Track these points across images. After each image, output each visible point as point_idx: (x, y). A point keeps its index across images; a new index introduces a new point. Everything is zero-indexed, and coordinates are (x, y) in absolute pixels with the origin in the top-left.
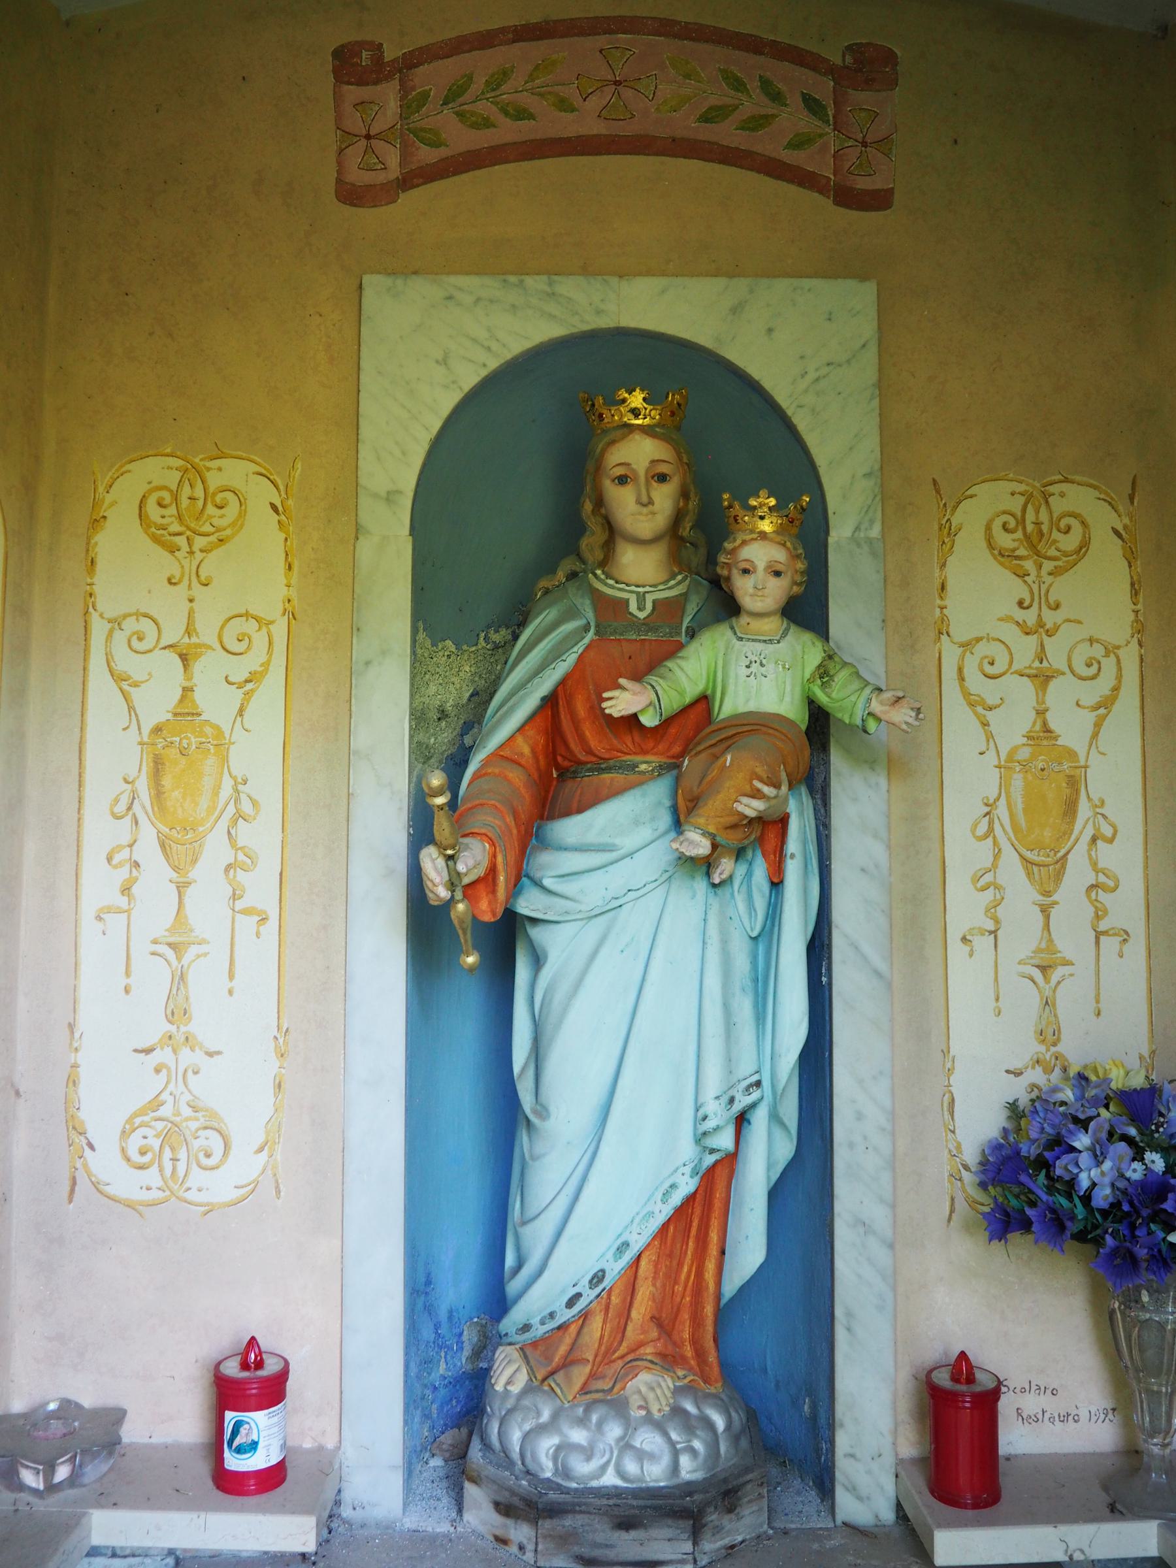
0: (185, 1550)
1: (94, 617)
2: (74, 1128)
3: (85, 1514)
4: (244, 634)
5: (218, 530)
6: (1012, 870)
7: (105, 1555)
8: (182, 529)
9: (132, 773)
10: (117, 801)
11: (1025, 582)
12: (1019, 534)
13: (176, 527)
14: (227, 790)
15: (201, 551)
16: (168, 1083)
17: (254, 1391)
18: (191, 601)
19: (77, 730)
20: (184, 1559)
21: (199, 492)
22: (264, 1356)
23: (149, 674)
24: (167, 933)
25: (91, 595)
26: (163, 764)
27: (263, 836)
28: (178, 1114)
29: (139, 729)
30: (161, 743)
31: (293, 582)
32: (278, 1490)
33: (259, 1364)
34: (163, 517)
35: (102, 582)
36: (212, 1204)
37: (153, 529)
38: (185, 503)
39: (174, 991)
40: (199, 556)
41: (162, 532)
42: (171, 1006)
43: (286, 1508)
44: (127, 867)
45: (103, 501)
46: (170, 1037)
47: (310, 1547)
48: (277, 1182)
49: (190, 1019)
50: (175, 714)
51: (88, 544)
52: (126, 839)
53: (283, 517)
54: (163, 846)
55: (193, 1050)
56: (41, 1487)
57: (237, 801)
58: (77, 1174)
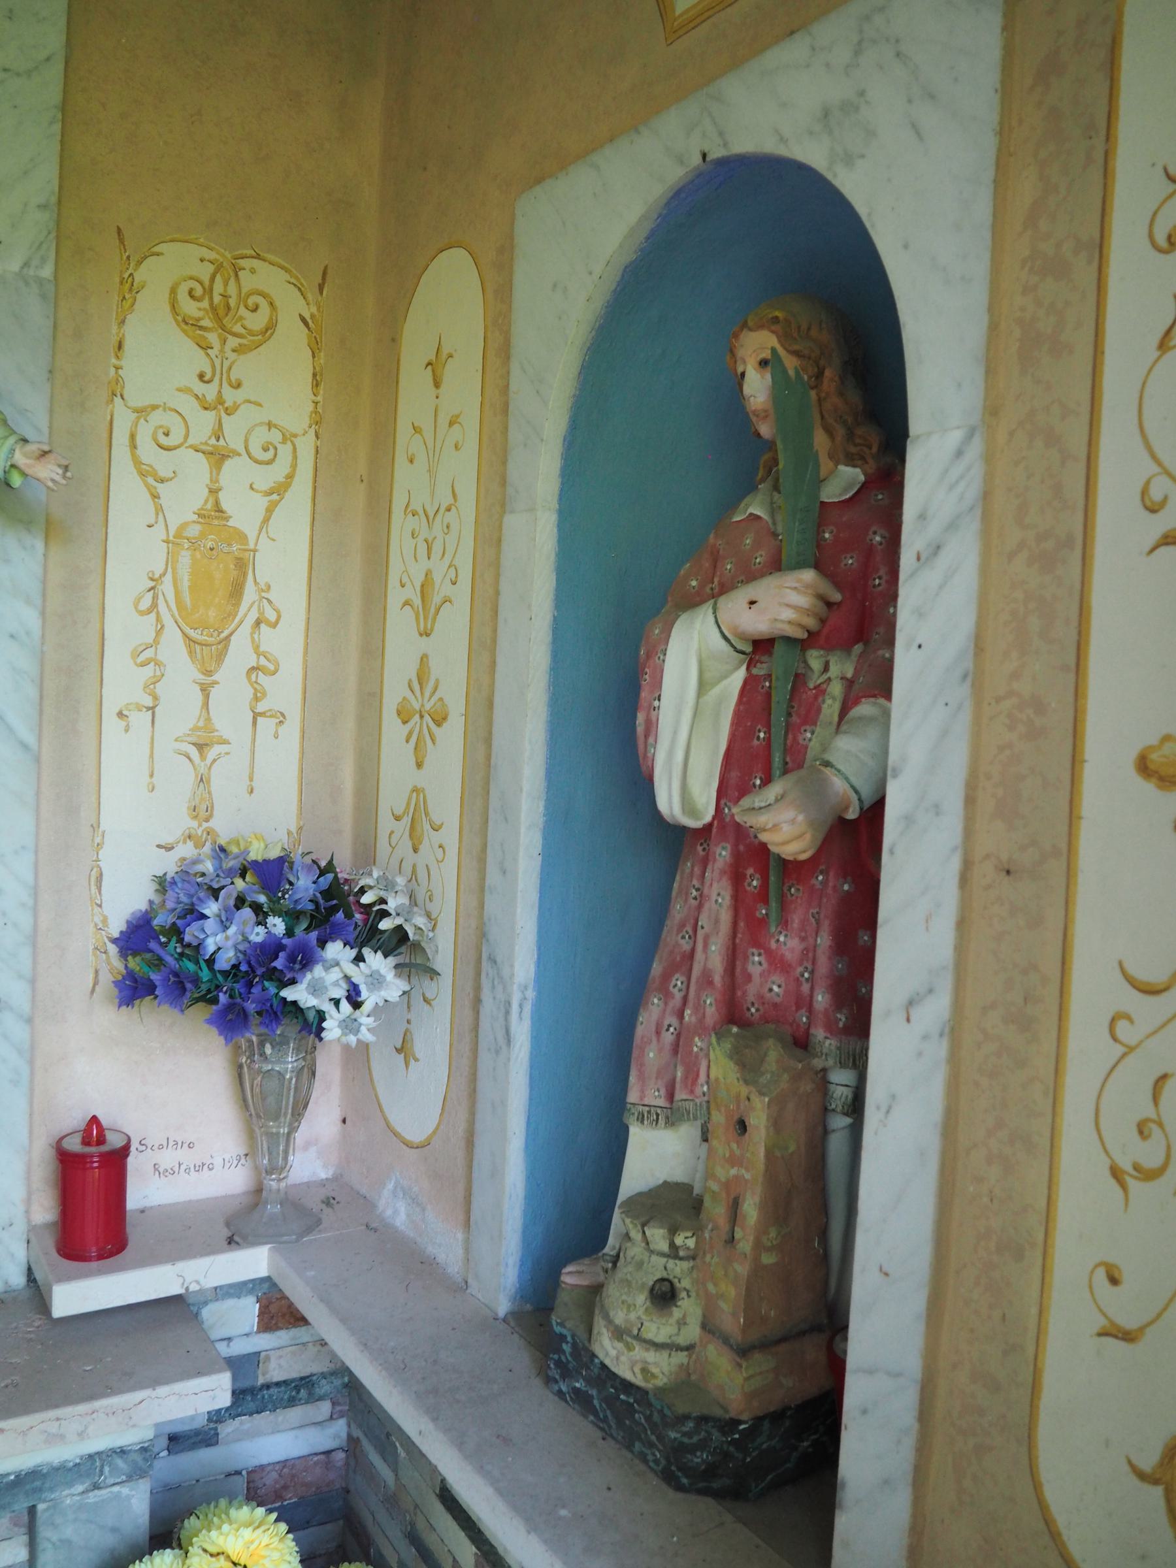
6: (173, 647)
11: (208, 354)
12: (205, 304)
15: (234, 351)
27: (287, 643)
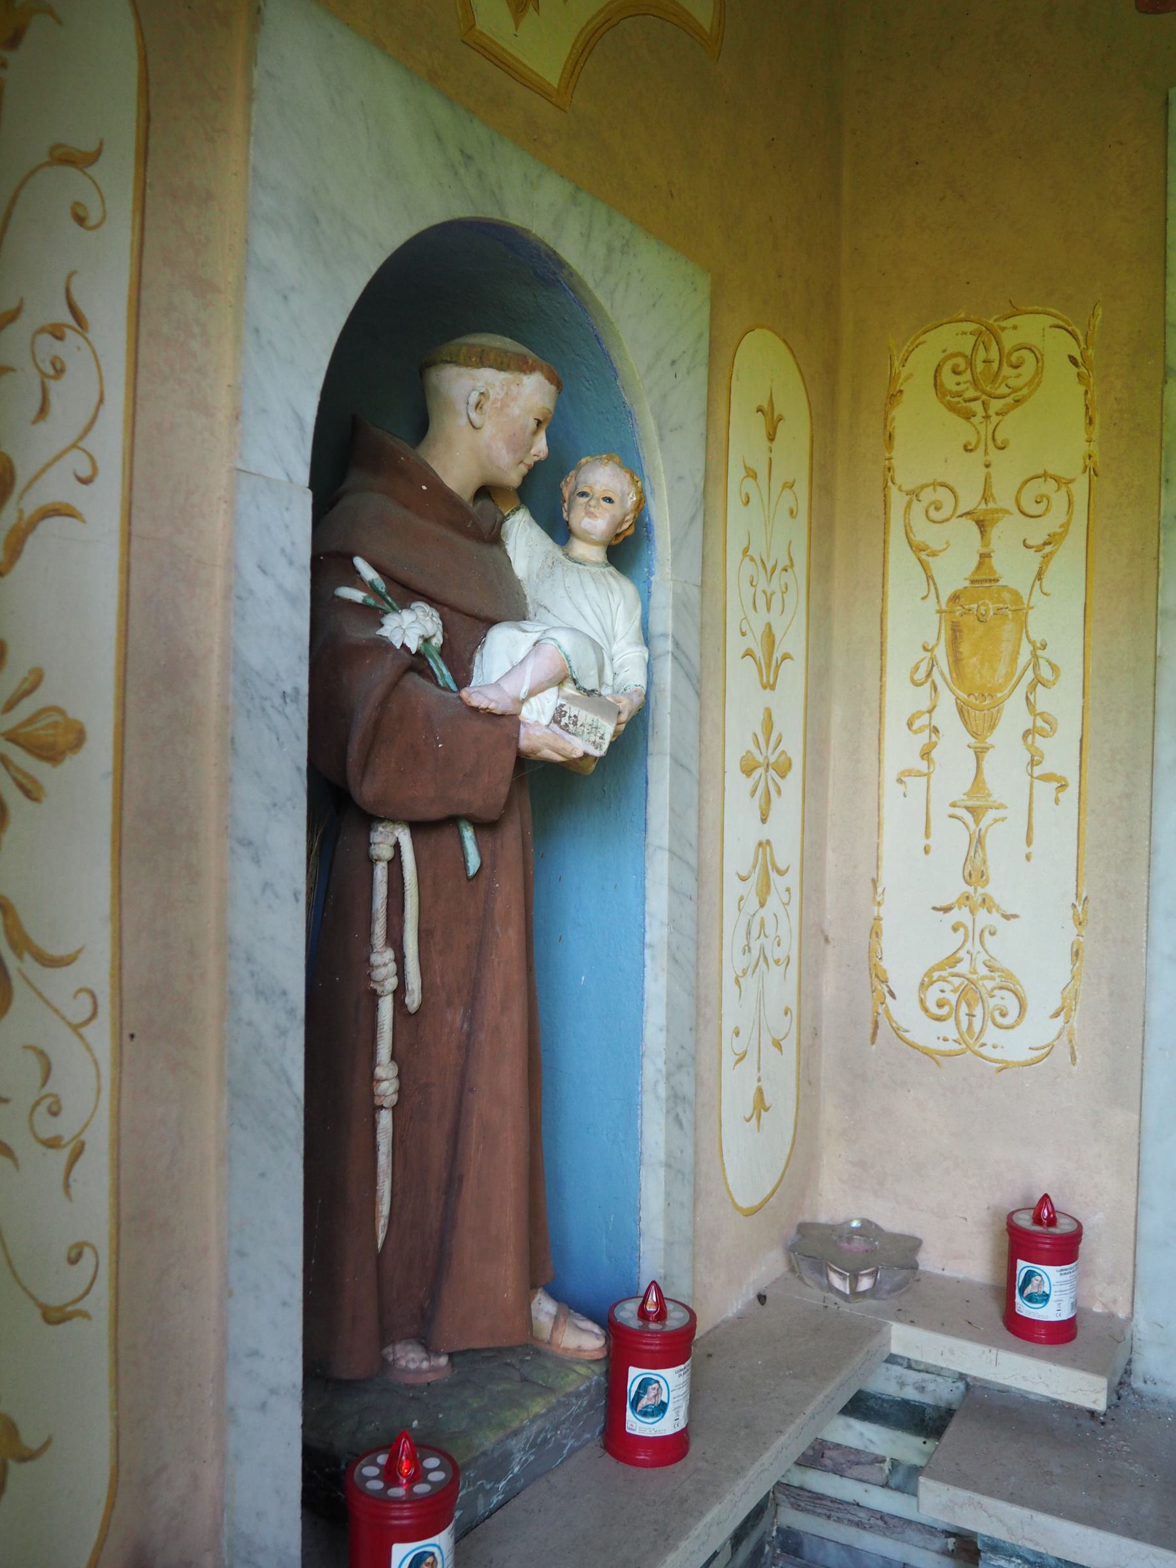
0: (975, 1378)
1: (894, 492)
2: (877, 976)
3: (885, 1324)
4: (1042, 496)
5: (1015, 390)
7: (901, 1365)
8: (978, 394)
9: (931, 643)
10: (916, 668)
13: (971, 393)
14: (1025, 656)
15: (997, 414)
16: (965, 941)
17: (1047, 1246)
18: (987, 466)
19: (879, 601)
20: (974, 1386)
21: (994, 354)
22: (1057, 1215)
23: (948, 543)
24: (965, 797)
25: (889, 469)
26: (961, 631)
27: (1064, 701)
28: (975, 972)
29: (938, 597)
30: (958, 610)
31: (1095, 436)
32: (1068, 1344)
33: (1052, 1222)
34: (958, 384)
35: (899, 455)
36: (1006, 1062)
37: (948, 398)
38: (980, 366)
39: (972, 854)
40: (995, 419)
41: (957, 399)
42: (969, 867)
43: (1073, 1363)
44: (927, 732)
45: (900, 373)
46: (967, 898)
47: (1101, 1406)
48: (1072, 1047)
49: (987, 882)
50: (973, 582)
51: (886, 419)
52: (925, 705)
53: (1083, 369)
54: (961, 712)
55: (989, 911)
56: (848, 1292)
57: (1036, 667)
58: (879, 1018)
